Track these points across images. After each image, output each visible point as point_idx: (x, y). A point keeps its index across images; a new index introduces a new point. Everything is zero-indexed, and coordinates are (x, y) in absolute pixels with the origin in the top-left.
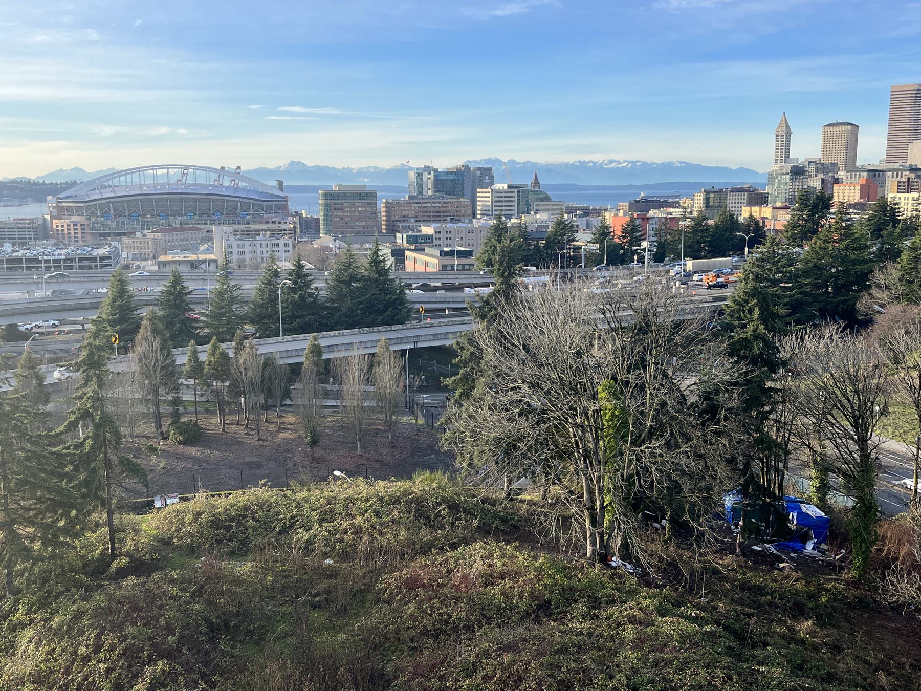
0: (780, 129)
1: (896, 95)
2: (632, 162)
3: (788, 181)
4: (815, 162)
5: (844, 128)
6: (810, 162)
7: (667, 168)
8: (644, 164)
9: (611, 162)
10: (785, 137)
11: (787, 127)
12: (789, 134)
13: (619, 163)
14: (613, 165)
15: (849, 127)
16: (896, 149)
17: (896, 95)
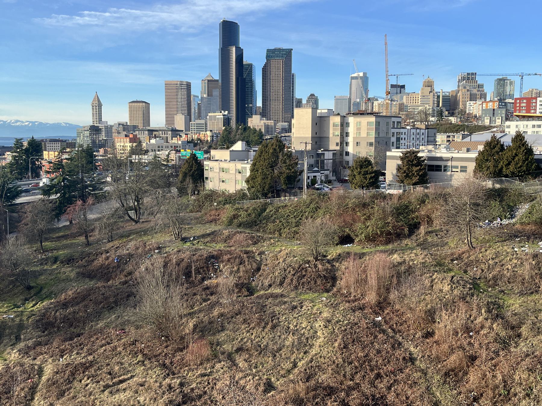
0: (94, 102)
1: (168, 86)
2: (30, 122)
3: (88, 135)
4: (123, 125)
5: (141, 104)
6: (119, 124)
7: (57, 126)
8: (41, 124)
9: (17, 121)
10: (98, 107)
11: (99, 101)
12: (100, 105)
13: (22, 122)
14: (18, 124)
15: (144, 104)
16: (170, 118)
17: (168, 86)
